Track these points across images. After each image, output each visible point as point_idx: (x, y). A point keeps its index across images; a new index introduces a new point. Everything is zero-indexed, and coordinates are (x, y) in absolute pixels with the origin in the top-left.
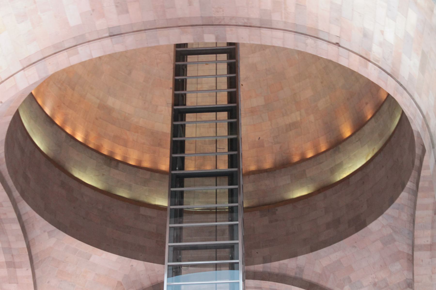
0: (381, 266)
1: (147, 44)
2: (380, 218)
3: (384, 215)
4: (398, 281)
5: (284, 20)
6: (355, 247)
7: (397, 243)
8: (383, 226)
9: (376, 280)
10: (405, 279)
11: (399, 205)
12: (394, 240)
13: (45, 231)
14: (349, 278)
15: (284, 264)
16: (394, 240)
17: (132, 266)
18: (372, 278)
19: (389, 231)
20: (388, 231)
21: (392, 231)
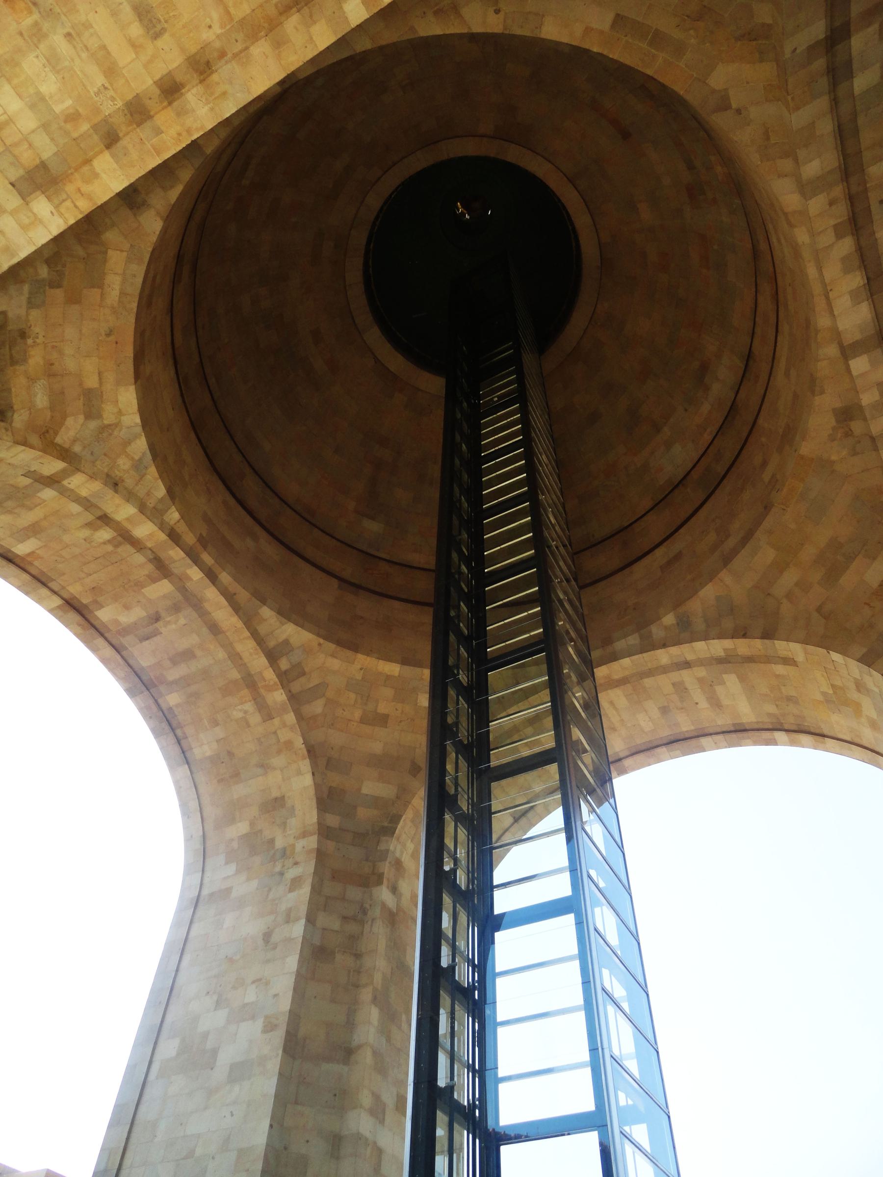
0: (52, 364)
1: (643, 657)
2: (138, 420)
3: (139, 429)
4: (13, 390)
5: (521, 733)
6: (108, 335)
7: (81, 419)
8: (120, 413)
9: (30, 341)
10: (15, 407)
11: (146, 468)
12: (89, 416)
13: (739, 111)
14: (59, 286)
15: (172, 187)
16: (89, 416)
17: (497, 12)
18: (37, 333)
19: (109, 417)
20: (109, 415)
21: (106, 422)
